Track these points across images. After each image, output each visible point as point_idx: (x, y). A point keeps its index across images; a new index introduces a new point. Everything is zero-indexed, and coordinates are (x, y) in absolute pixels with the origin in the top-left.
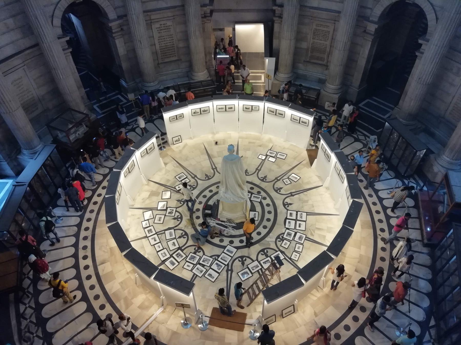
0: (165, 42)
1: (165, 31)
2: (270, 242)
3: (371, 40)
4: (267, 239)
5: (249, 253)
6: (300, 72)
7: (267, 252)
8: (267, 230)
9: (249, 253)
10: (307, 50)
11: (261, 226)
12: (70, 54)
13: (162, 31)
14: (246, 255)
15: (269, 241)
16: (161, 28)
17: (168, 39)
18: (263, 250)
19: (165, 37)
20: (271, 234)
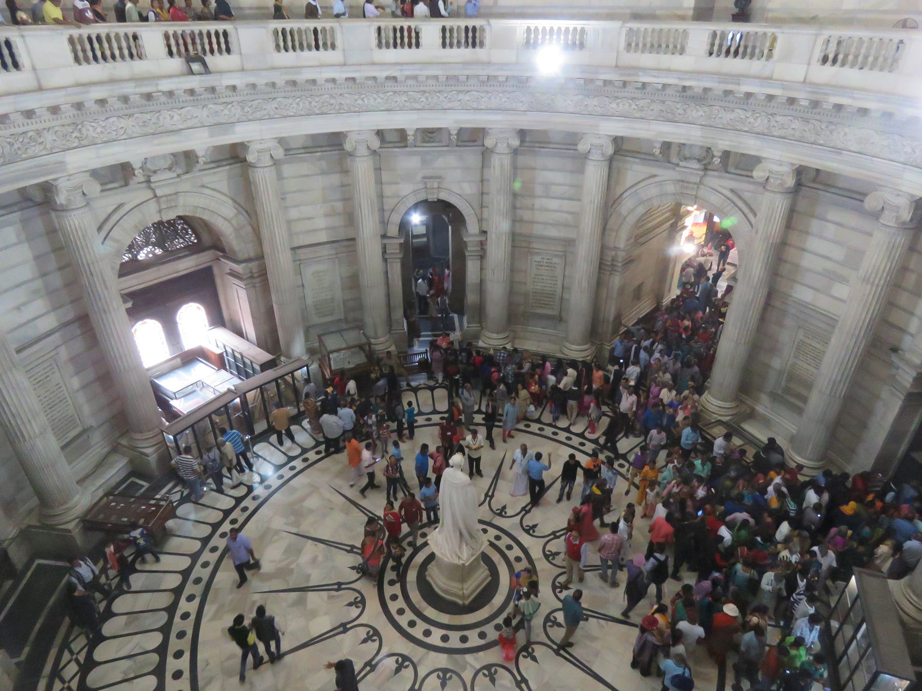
0: (544, 285)
1: (547, 268)
2: (468, 666)
3: (903, 397)
4: (469, 658)
5: (420, 661)
6: (760, 409)
7: (451, 678)
8: (482, 642)
9: (420, 661)
10: (781, 372)
11: (478, 630)
12: (399, 260)
13: (542, 268)
14: (415, 660)
15: (467, 662)
16: (542, 263)
17: (549, 282)
18: (445, 671)
19: (545, 278)
20: (481, 653)
